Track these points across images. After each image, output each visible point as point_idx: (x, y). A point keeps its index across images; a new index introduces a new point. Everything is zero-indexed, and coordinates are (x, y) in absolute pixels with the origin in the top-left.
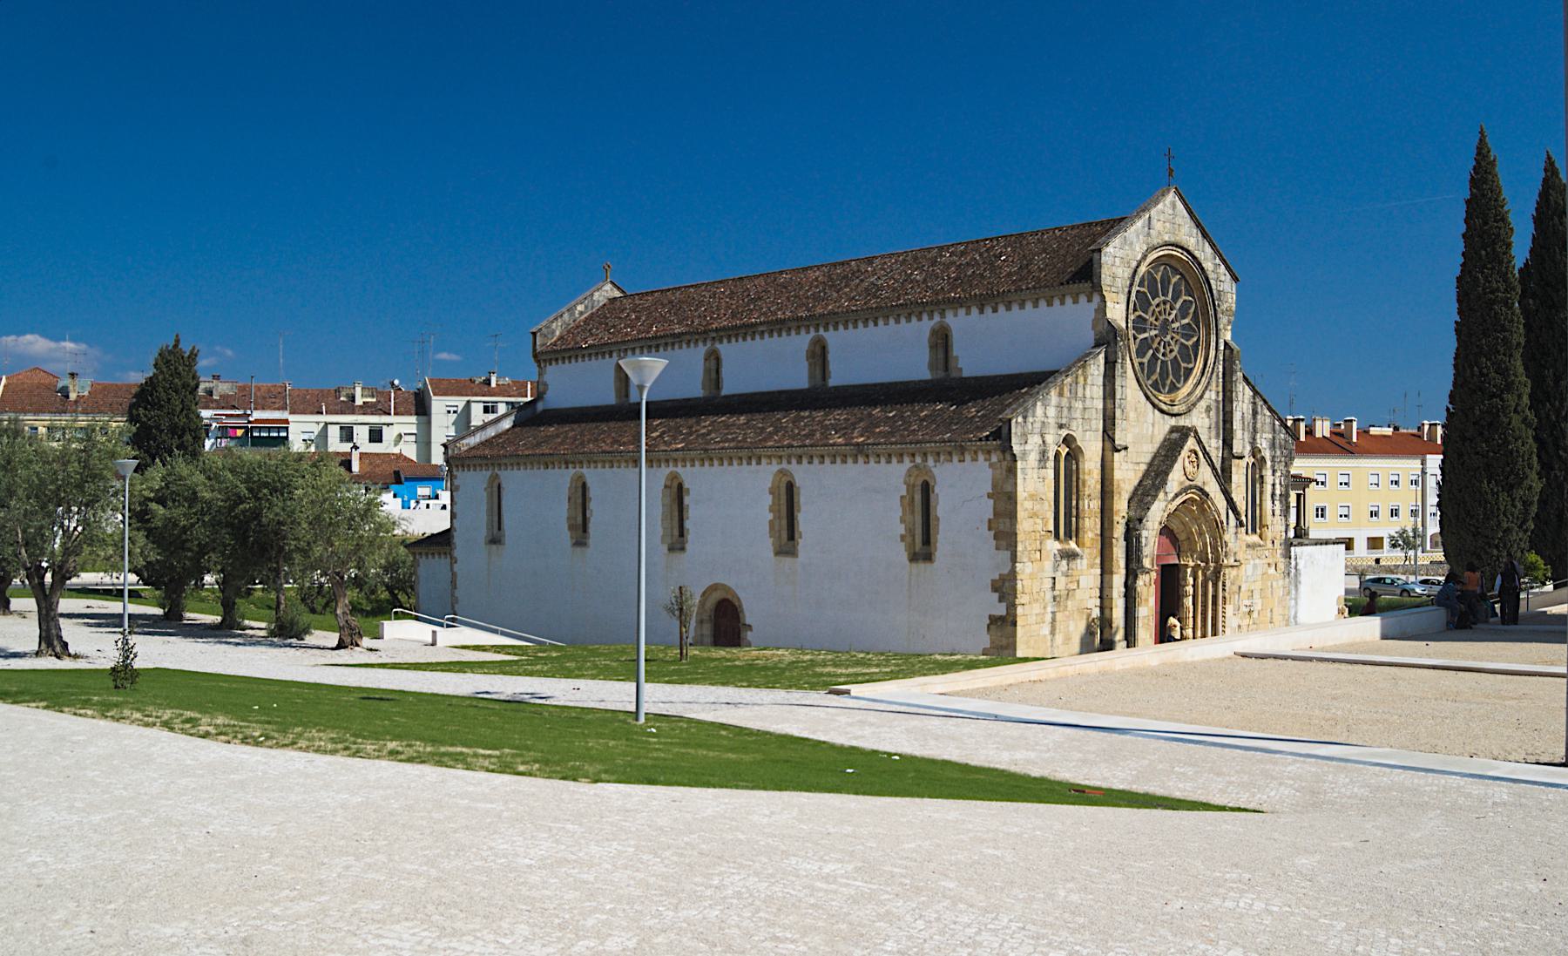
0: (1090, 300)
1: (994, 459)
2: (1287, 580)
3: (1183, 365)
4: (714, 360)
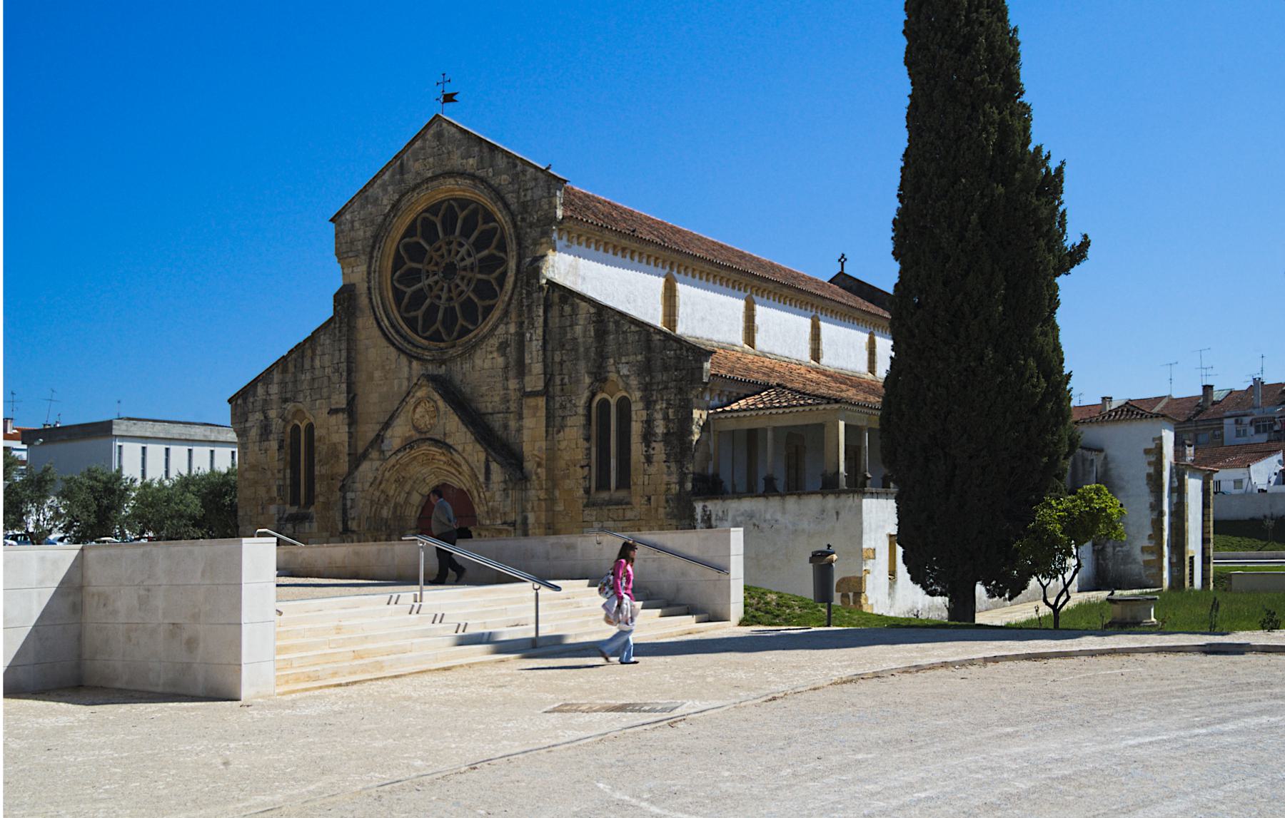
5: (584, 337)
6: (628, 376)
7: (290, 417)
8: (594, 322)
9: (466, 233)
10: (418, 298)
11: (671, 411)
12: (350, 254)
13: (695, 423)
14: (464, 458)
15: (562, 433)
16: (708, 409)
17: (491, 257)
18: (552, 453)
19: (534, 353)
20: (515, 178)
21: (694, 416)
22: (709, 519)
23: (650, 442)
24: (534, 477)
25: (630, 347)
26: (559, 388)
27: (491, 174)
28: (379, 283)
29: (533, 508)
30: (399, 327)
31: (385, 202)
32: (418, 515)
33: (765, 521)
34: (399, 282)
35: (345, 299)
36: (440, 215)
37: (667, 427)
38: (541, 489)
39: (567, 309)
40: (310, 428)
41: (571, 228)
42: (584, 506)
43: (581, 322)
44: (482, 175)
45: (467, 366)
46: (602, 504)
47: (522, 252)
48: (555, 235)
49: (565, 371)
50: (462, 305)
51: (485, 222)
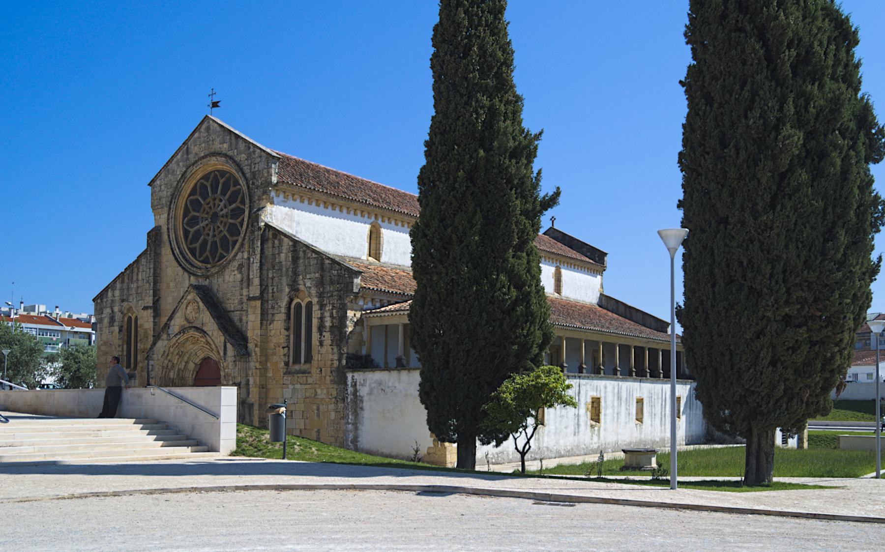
2: (341, 405)
5: (286, 261)
6: (310, 288)
7: (125, 312)
8: (291, 251)
9: (224, 193)
10: (197, 234)
11: (334, 311)
12: (159, 207)
13: (349, 319)
14: (212, 340)
15: (272, 325)
16: (362, 310)
17: (238, 208)
18: (265, 338)
19: (255, 271)
20: (249, 156)
21: (348, 315)
22: (355, 385)
23: (322, 332)
24: (253, 354)
25: (311, 268)
26: (270, 295)
27: (236, 154)
28: (174, 225)
29: (252, 374)
30: (185, 254)
31: (178, 173)
32: (194, 377)
33: (388, 387)
34: (187, 224)
35: (154, 236)
36: (210, 180)
37: (332, 322)
38: (257, 361)
39: (277, 242)
40: (136, 318)
41: (285, 189)
42: (284, 374)
43: (284, 251)
44: (231, 154)
45: (220, 280)
46: (294, 373)
47: (252, 205)
48: (273, 194)
49: (275, 284)
50: (221, 240)
51: (235, 186)
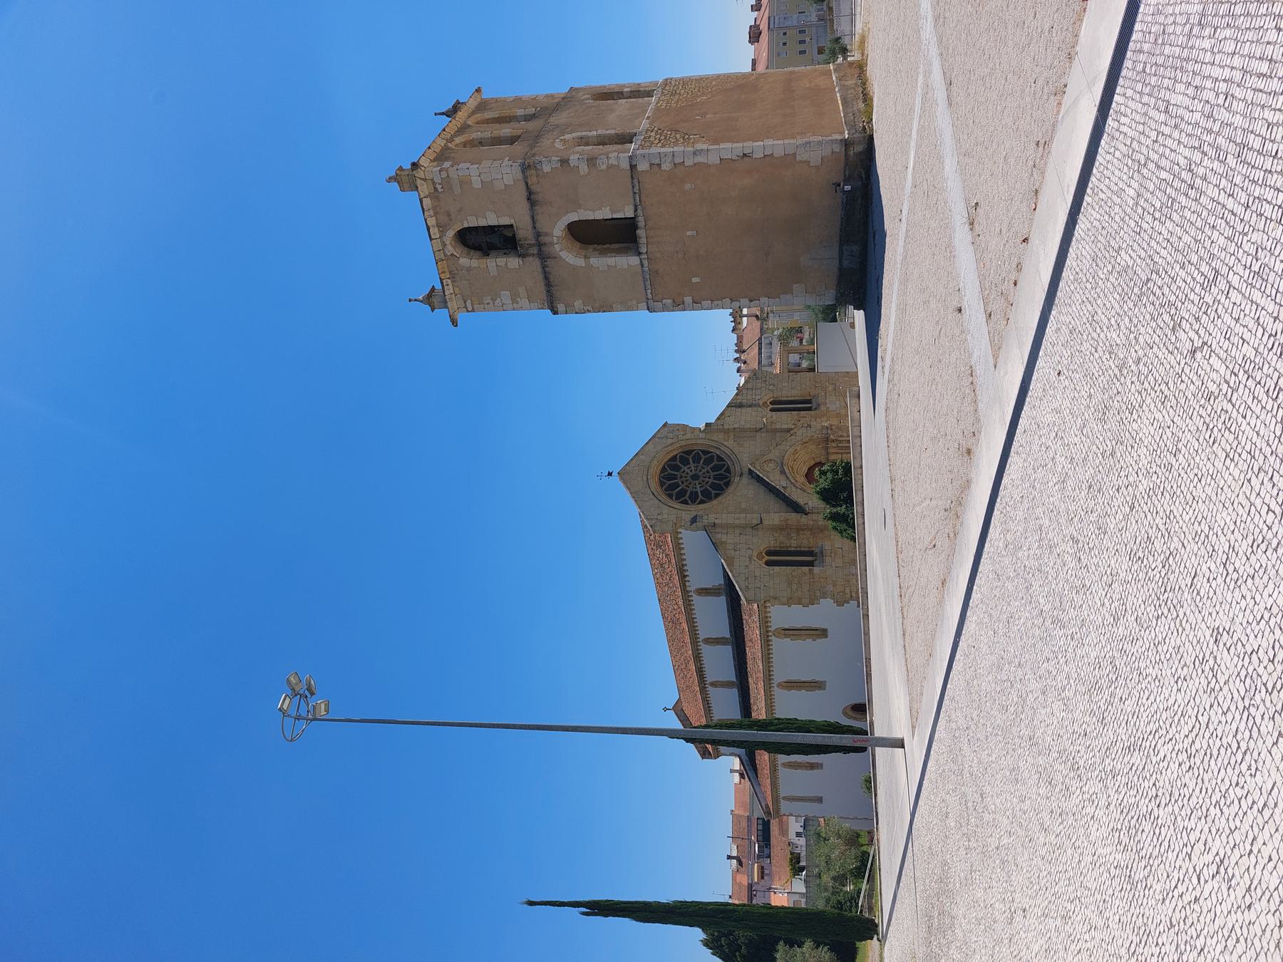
0: (681, 533)
1: (769, 605)
3: (715, 462)
4: (704, 592)
40: (769, 553)
